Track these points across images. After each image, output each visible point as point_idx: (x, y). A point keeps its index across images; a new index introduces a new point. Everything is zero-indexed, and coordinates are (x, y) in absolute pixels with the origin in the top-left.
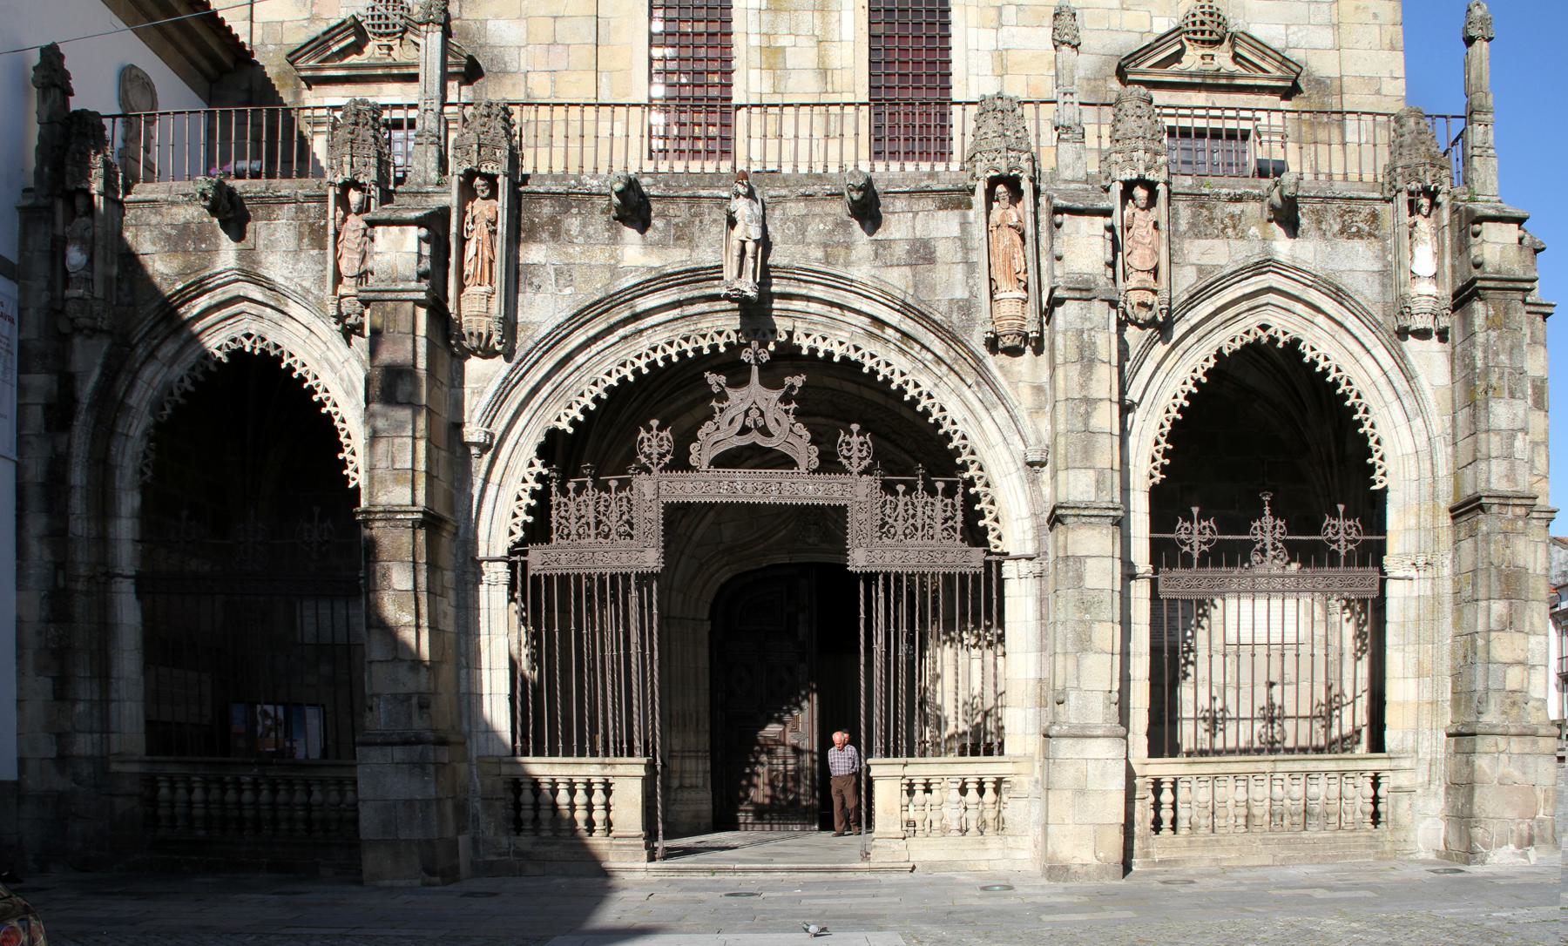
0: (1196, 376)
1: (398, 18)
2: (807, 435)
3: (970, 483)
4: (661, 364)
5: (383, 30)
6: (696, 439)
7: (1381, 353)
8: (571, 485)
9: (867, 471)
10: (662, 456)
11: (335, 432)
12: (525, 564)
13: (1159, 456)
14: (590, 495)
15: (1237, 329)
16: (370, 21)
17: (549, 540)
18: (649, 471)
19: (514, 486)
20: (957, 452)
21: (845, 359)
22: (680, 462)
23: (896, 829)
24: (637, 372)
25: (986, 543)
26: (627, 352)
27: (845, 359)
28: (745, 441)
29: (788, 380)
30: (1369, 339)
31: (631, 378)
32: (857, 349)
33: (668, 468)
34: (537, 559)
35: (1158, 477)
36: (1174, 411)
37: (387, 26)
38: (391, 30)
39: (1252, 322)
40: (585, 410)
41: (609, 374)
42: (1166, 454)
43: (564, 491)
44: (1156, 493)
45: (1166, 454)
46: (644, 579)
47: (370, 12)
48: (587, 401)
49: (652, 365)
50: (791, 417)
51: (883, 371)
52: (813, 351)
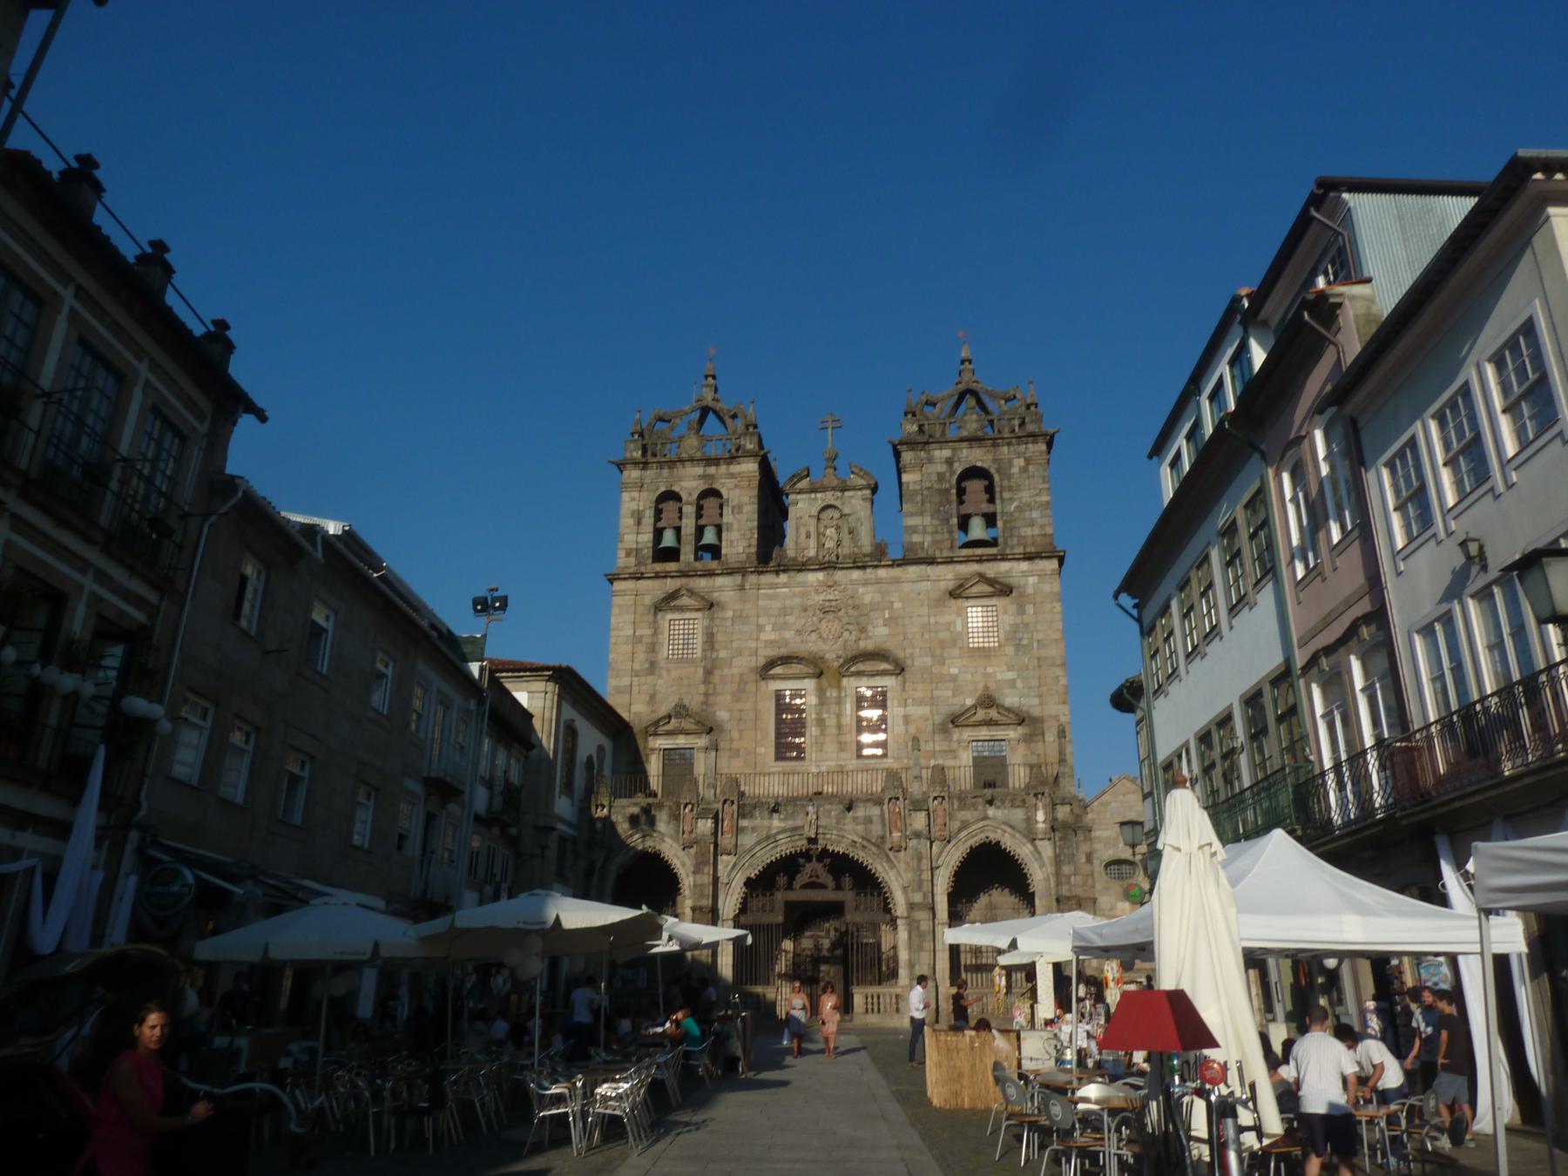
3: (886, 893)
7: (1029, 845)
11: (677, 879)
14: (760, 897)
19: (736, 896)
20: (880, 883)
21: (843, 853)
22: (790, 887)
23: (862, 1010)
26: (773, 852)
28: (812, 880)
30: (1024, 840)
33: (786, 889)
39: (982, 836)
43: (752, 897)
44: (949, 895)
46: (778, 925)
48: (760, 868)
52: (833, 851)
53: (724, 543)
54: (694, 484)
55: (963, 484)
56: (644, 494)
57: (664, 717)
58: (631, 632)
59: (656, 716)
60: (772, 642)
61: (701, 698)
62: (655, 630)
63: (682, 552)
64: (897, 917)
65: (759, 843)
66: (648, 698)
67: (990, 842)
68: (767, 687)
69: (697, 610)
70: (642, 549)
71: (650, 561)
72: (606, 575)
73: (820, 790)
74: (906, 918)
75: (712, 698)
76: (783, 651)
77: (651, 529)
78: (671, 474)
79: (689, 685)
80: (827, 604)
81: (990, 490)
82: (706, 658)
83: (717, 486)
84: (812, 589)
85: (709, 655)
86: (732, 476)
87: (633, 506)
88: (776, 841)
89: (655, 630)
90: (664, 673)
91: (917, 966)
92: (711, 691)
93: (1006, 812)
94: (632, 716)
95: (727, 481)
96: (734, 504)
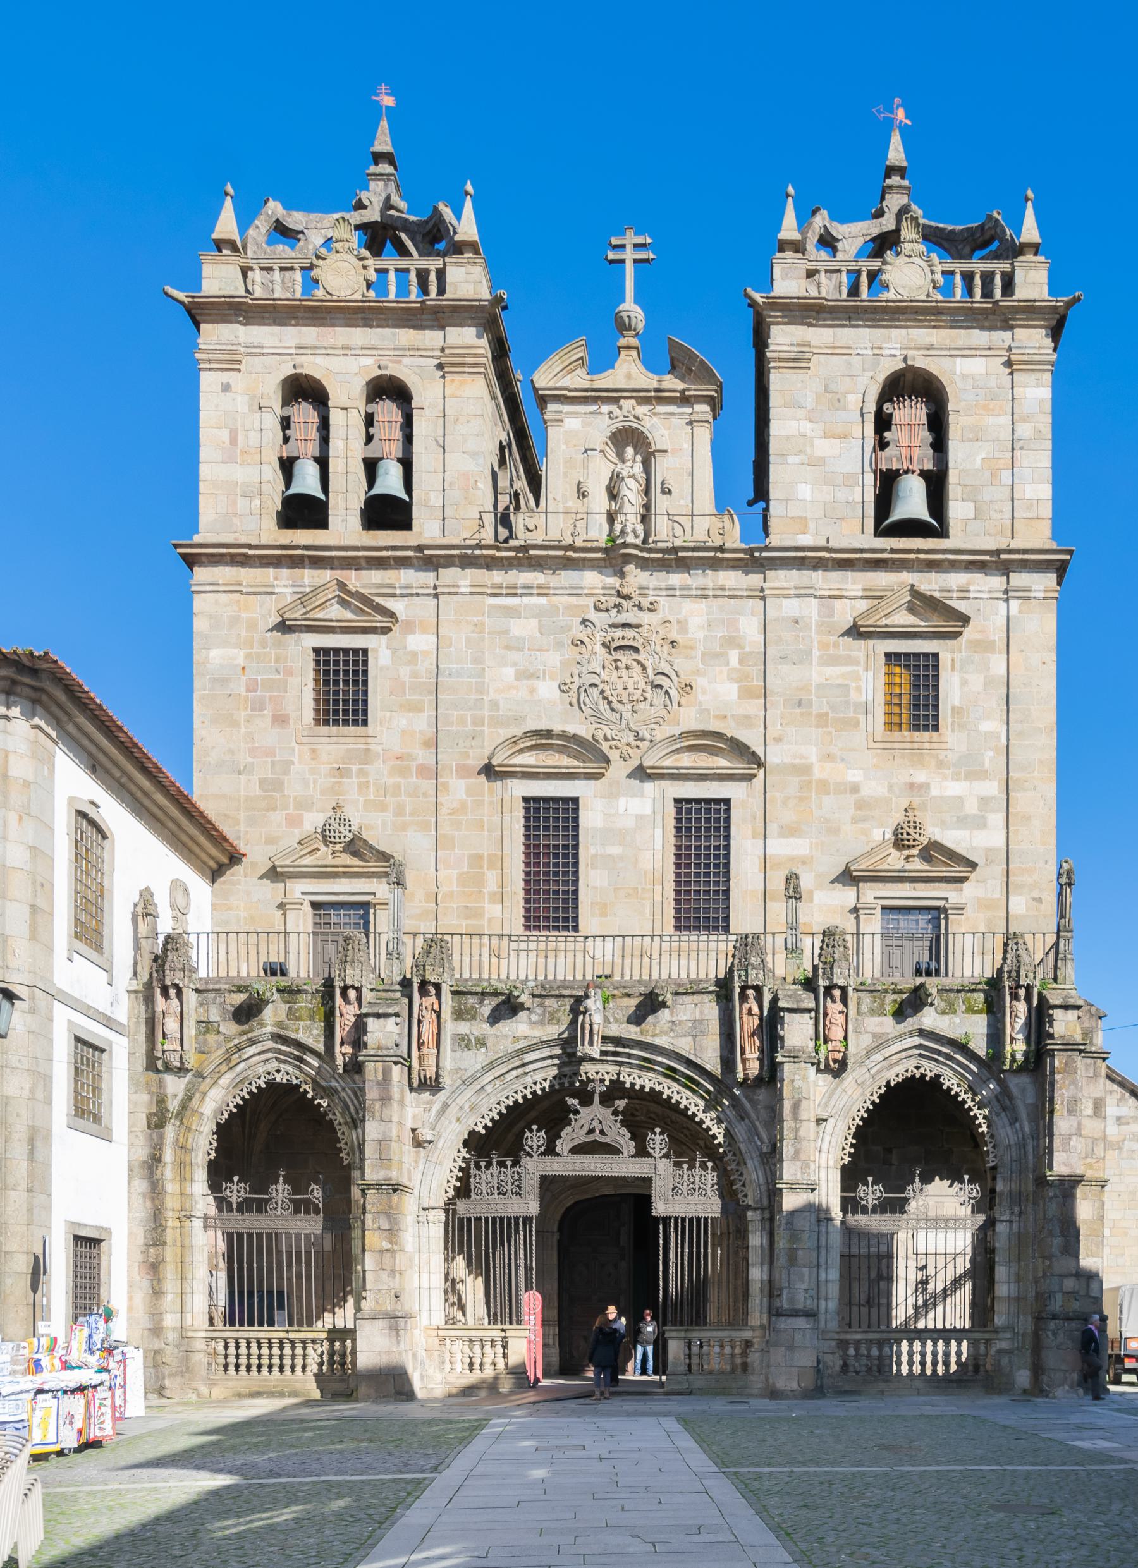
0: (872, 1098)
2: (629, 1135)
4: (539, 1092)
6: (560, 1137)
8: (483, 1164)
9: (666, 1156)
10: (539, 1147)
12: (454, 1211)
13: (847, 1147)
14: (494, 1169)
15: (900, 1069)
17: (469, 1197)
18: (531, 1156)
21: (652, 1089)
22: (550, 1150)
24: (524, 1097)
25: (738, 1200)
27: (652, 1089)
28: (590, 1138)
29: (617, 1103)
31: (521, 1101)
32: (659, 1084)
33: (542, 1154)
34: (463, 1208)
35: (847, 1160)
36: (857, 1119)
39: (910, 1064)
40: (492, 1120)
41: (507, 1098)
42: (852, 1145)
43: (478, 1167)
44: (844, 1169)
45: (852, 1145)
46: (527, 1220)
49: (534, 1093)
50: (619, 1125)
51: (676, 1097)
52: (633, 1085)
55: (887, 407)
64: (749, 1207)
65: (491, 1066)
67: (923, 1076)
73: (608, 972)
74: (763, 1209)
80: (619, 633)
81: (938, 425)
88: (524, 1065)
91: (785, 1292)
93: (957, 1020)
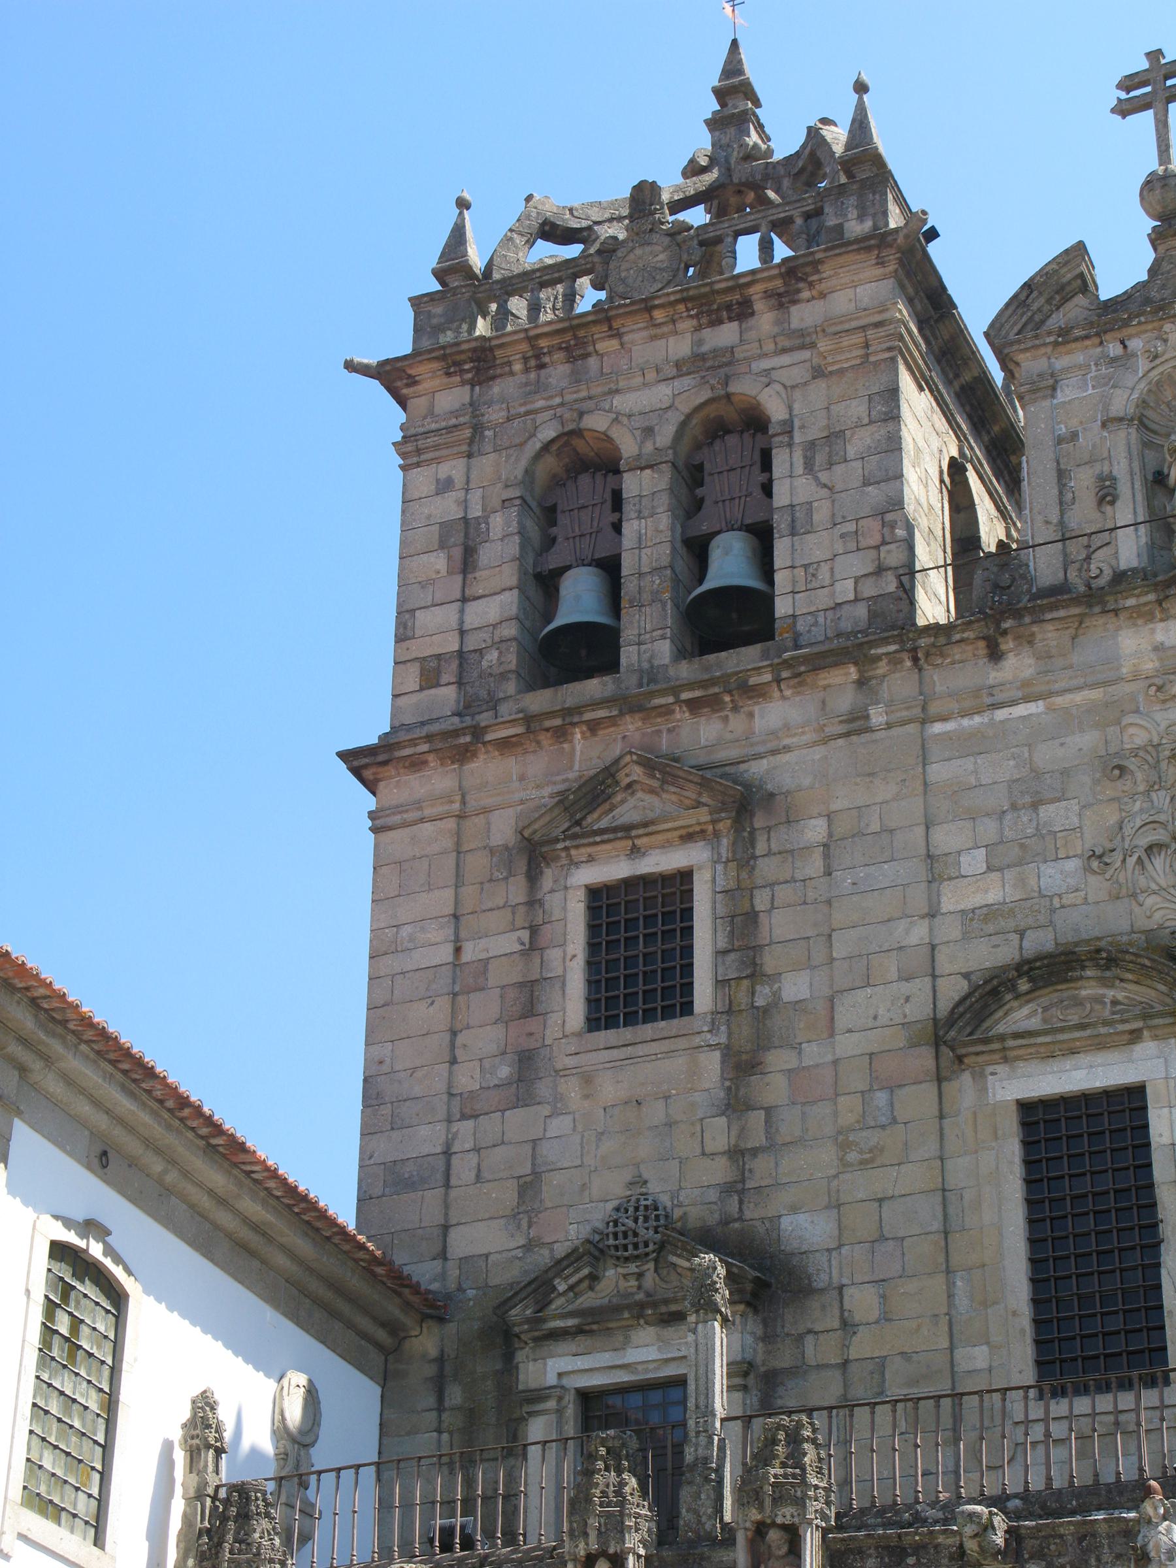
1: (651, 1232)
5: (631, 1251)
16: (611, 1242)
37: (636, 1246)
38: (641, 1250)
47: (611, 1229)
53: (779, 577)
54: (663, 393)
56: (486, 464)
57: (573, 1258)
58: (445, 954)
59: (543, 1258)
60: (990, 913)
61: (719, 1171)
62: (534, 930)
63: (628, 633)
66: (508, 1195)
68: (984, 1090)
69: (689, 837)
70: (480, 652)
71: (511, 687)
72: (344, 756)
75: (761, 1167)
76: (1040, 941)
77: (509, 575)
78: (577, 378)
79: (670, 1124)
82: (729, 1011)
83: (744, 387)
84: (1140, 685)
85: (742, 998)
86: (803, 340)
87: (447, 508)
89: (534, 930)
90: (571, 1089)
92: (757, 1139)
94: (453, 1273)
95: (785, 359)
96: (815, 432)
